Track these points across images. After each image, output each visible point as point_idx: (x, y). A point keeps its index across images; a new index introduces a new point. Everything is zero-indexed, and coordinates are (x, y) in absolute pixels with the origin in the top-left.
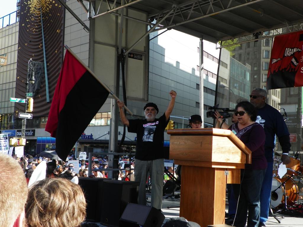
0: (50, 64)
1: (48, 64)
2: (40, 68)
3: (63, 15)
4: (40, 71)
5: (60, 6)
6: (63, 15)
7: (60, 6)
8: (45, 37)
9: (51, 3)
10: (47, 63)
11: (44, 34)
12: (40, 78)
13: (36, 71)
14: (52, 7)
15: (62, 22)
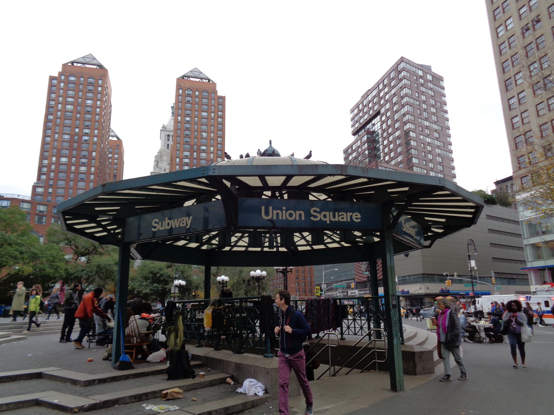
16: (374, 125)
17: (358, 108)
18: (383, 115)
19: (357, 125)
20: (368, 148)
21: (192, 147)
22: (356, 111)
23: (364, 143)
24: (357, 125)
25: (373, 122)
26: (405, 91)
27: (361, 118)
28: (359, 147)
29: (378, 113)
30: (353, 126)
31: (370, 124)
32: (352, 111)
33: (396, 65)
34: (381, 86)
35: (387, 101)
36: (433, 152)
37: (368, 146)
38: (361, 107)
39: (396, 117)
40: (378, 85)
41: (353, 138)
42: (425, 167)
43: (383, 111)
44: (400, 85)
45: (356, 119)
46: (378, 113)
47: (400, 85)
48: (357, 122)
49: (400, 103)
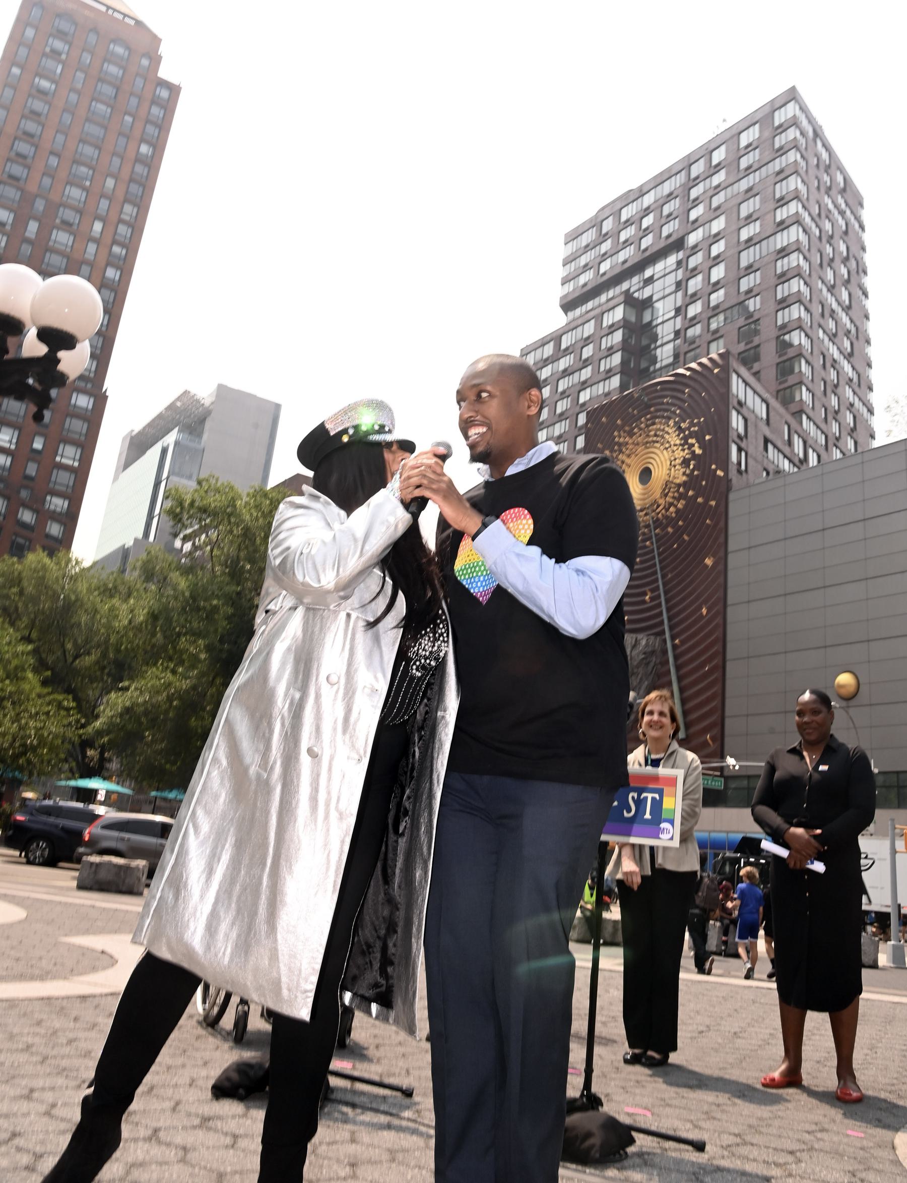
0: (683, 642)
1: (677, 641)
2: (653, 652)
3: (722, 524)
4: (654, 659)
5: (713, 503)
6: (722, 524)
7: (713, 503)
8: (663, 577)
9: (681, 497)
10: (673, 638)
11: (662, 569)
12: (651, 678)
13: (643, 659)
14: (686, 506)
15: (722, 540)
16: (650, 281)
17: (599, 229)
18: (695, 249)
19: (583, 279)
20: (625, 346)
21: (27, 199)
22: (585, 239)
23: (612, 328)
24: (583, 279)
25: (648, 273)
26: (794, 183)
27: (604, 257)
28: (587, 341)
29: (678, 244)
30: (565, 281)
31: (635, 279)
32: (573, 236)
33: (767, 110)
34: (697, 169)
35: (716, 212)
36: (839, 390)
37: (624, 341)
38: (607, 226)
39: (746, 258)
40: (688, 163)
41: (560, 320)
42: (823, 426)
43: (693, 239)
44: (777, 165)
45: (583, 260)
46: (678, 244)
47: (777, 165)
48: (586, 268)
49: (769, 217)
